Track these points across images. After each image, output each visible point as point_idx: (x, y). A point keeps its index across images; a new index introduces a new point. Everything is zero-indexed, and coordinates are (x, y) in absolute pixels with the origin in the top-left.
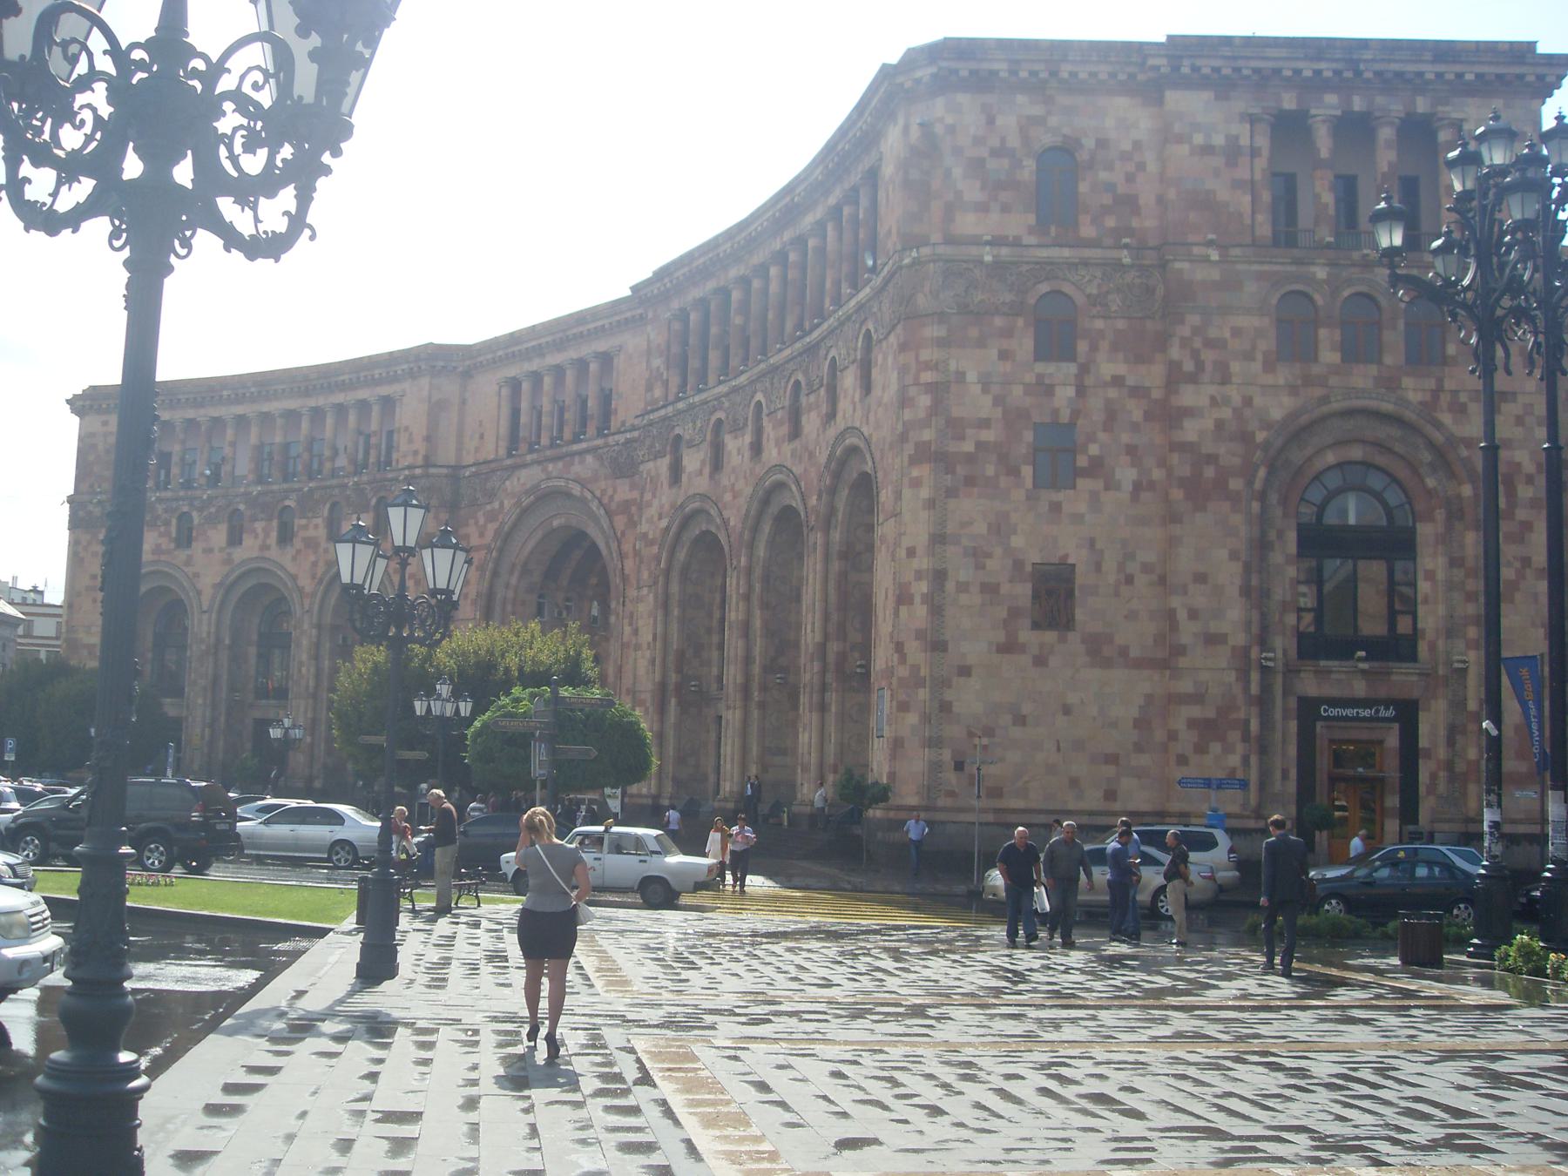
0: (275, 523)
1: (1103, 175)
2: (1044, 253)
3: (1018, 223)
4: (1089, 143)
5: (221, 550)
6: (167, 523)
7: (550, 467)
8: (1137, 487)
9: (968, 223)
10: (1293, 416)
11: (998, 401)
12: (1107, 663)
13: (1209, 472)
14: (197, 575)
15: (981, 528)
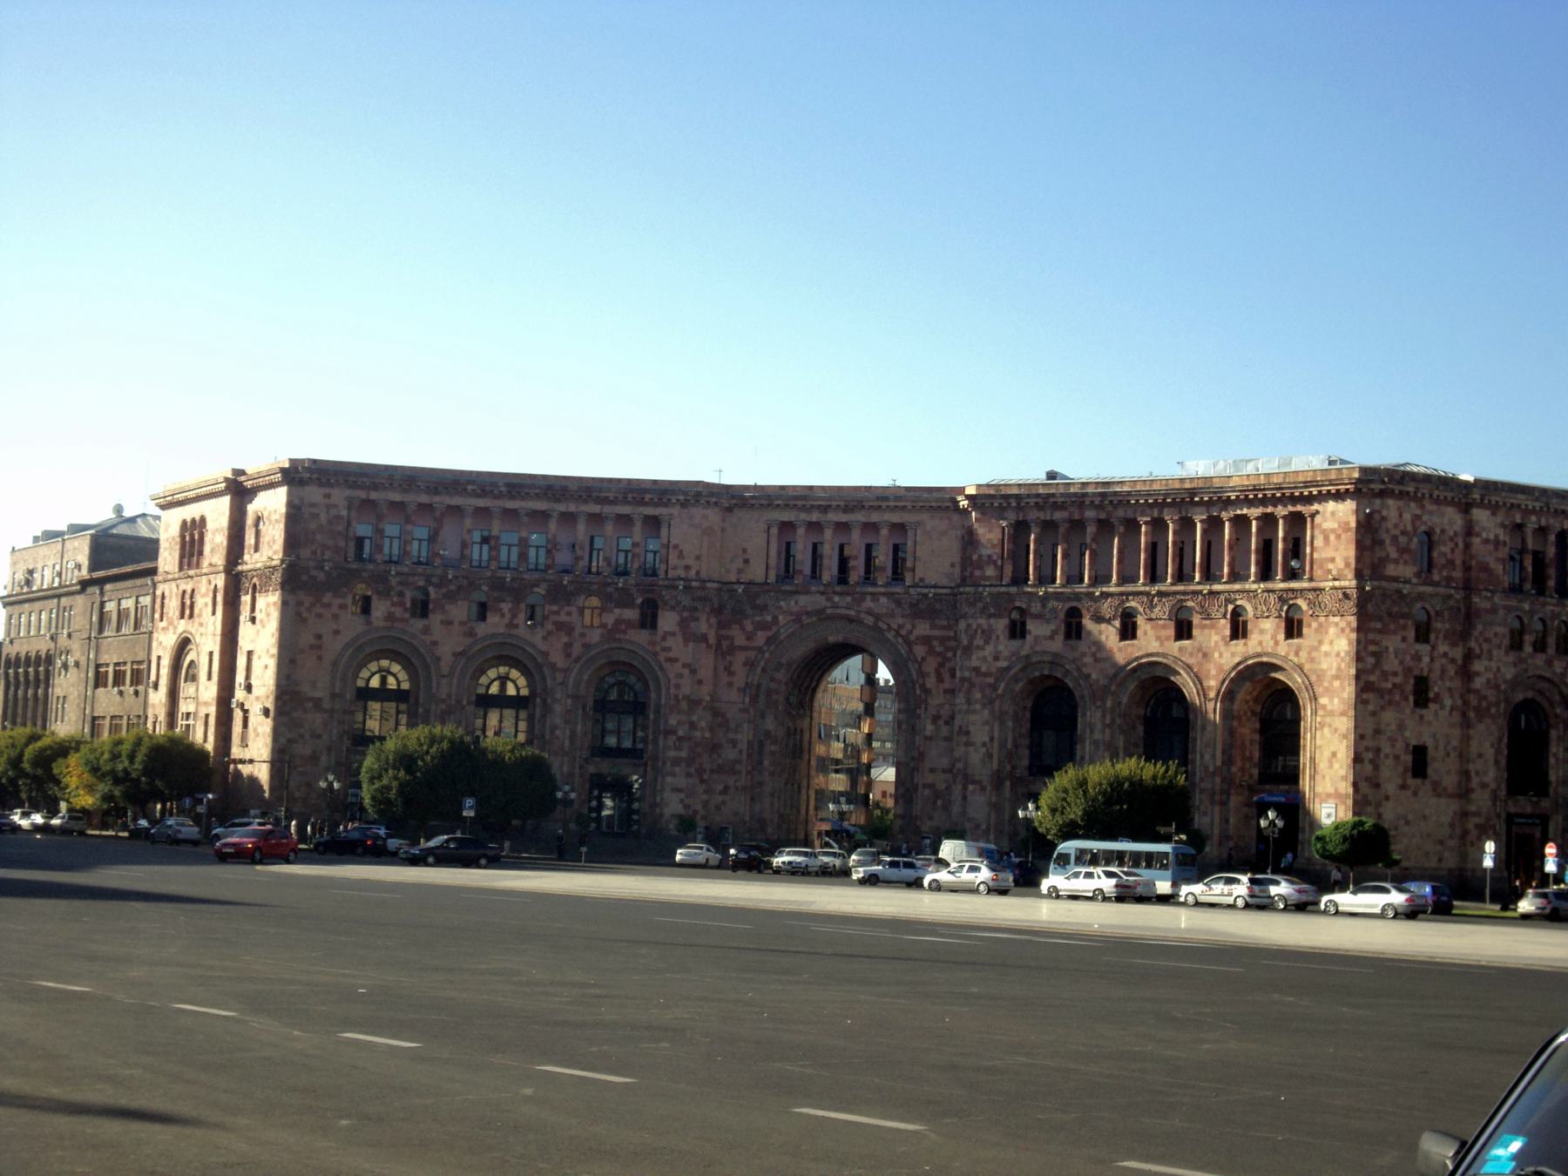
0: (523, 606)
1: (1443, 549)
2: (1422, 589)
3: (1407, 571)
4: (1438, 531)
5: (462, 623)
6: (401, 594)
7: (837, 599)
8: (1452, 709)
9: (1391, 570)
10: (1515, 677)
11: (1401, 663)
12: (1439, 795)
13: (1484, 704)
14: (435, 643)
15: (1393, 727)
